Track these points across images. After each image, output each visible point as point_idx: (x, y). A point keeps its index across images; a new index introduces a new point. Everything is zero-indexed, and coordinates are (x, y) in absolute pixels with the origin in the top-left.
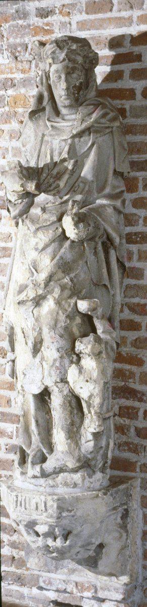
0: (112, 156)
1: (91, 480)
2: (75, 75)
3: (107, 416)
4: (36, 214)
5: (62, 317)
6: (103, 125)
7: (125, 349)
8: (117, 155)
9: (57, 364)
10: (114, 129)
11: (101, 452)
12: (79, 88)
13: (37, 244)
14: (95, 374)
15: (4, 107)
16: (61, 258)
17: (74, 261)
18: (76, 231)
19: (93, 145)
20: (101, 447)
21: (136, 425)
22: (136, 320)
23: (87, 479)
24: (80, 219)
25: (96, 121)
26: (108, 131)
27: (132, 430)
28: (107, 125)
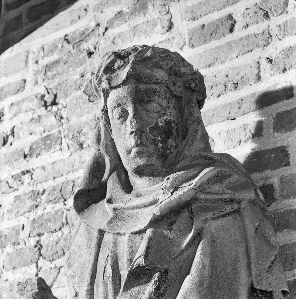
0: (242, 262)
2: (153, 106)
6: (217, 197)
8: (253, 255)
10: (244, 204)
12: (167, 131)
15: (60, 229)
19: (198, 237)
26: (230, 208)
28: (227, 196)
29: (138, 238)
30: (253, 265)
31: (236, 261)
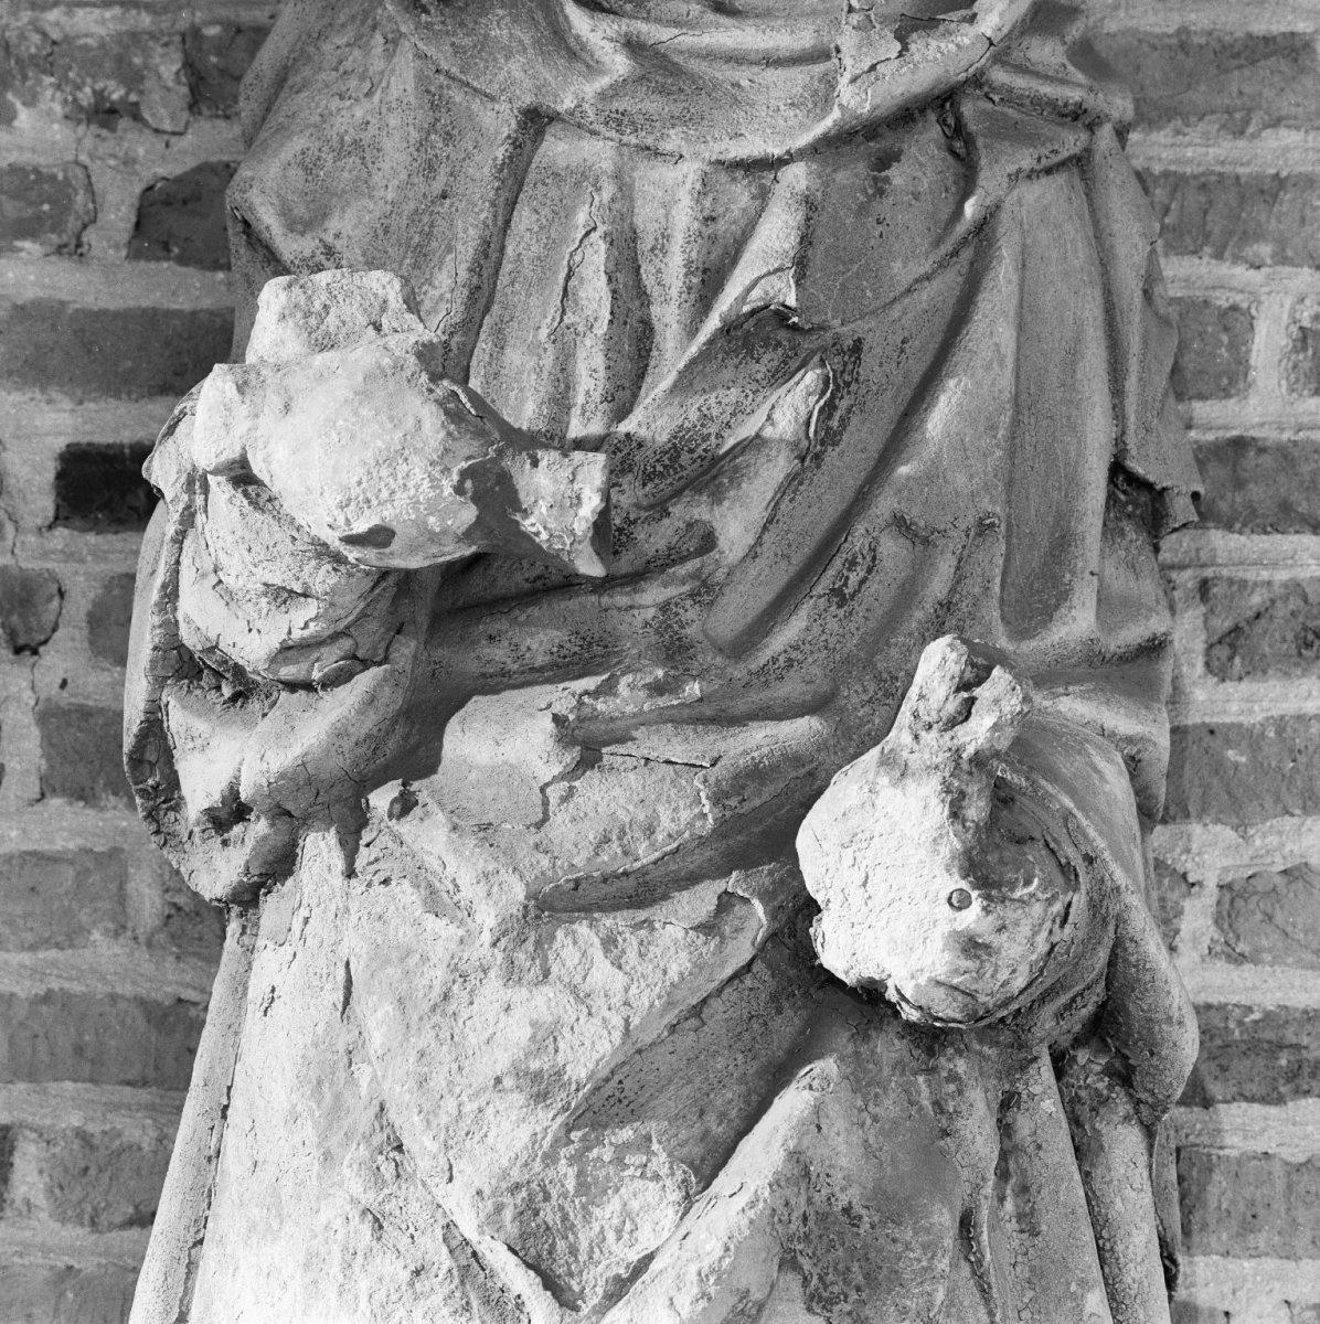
4: (506, 774)
6: (1047, 90)
13: (546, 1036)
16: (800, 1170)
17: (893, 1206)
18: (972, 917)
24: (1004, 827)
25: (1002, 51)
26: (1071, 141)
28: (1075, 95)
29: (741, 195)
30: (1132, 384)
31: (1073, 355)
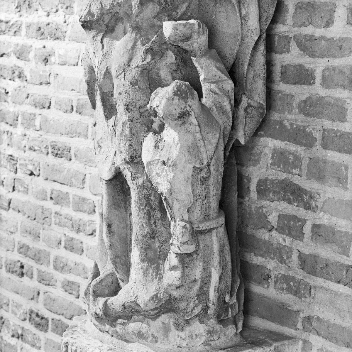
1: (182, 334)
3: (203, 226)
5: (141, 50)
7: (289, 116)
9: (127, 132)
11: (196, 288)
14: (175, 153)
20: (195, 281)
21: (299, 248)
22: (307, 66)
23: (174, 333)
27: (295, 256)
